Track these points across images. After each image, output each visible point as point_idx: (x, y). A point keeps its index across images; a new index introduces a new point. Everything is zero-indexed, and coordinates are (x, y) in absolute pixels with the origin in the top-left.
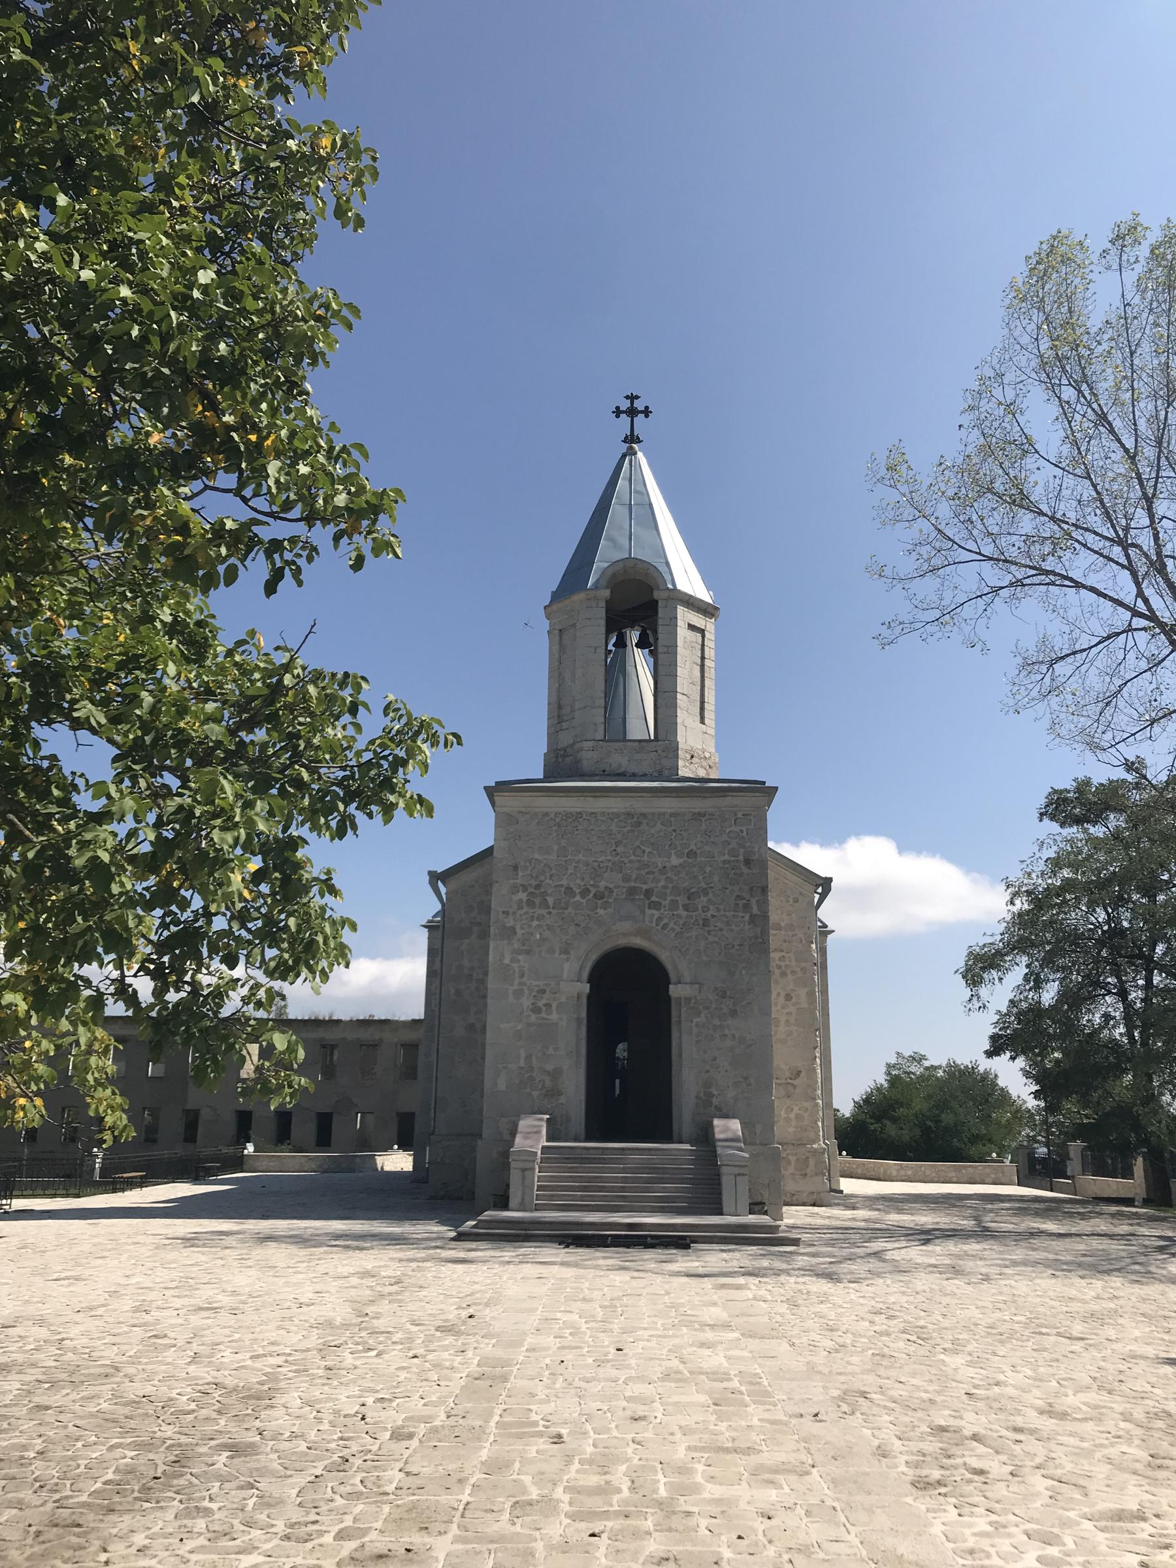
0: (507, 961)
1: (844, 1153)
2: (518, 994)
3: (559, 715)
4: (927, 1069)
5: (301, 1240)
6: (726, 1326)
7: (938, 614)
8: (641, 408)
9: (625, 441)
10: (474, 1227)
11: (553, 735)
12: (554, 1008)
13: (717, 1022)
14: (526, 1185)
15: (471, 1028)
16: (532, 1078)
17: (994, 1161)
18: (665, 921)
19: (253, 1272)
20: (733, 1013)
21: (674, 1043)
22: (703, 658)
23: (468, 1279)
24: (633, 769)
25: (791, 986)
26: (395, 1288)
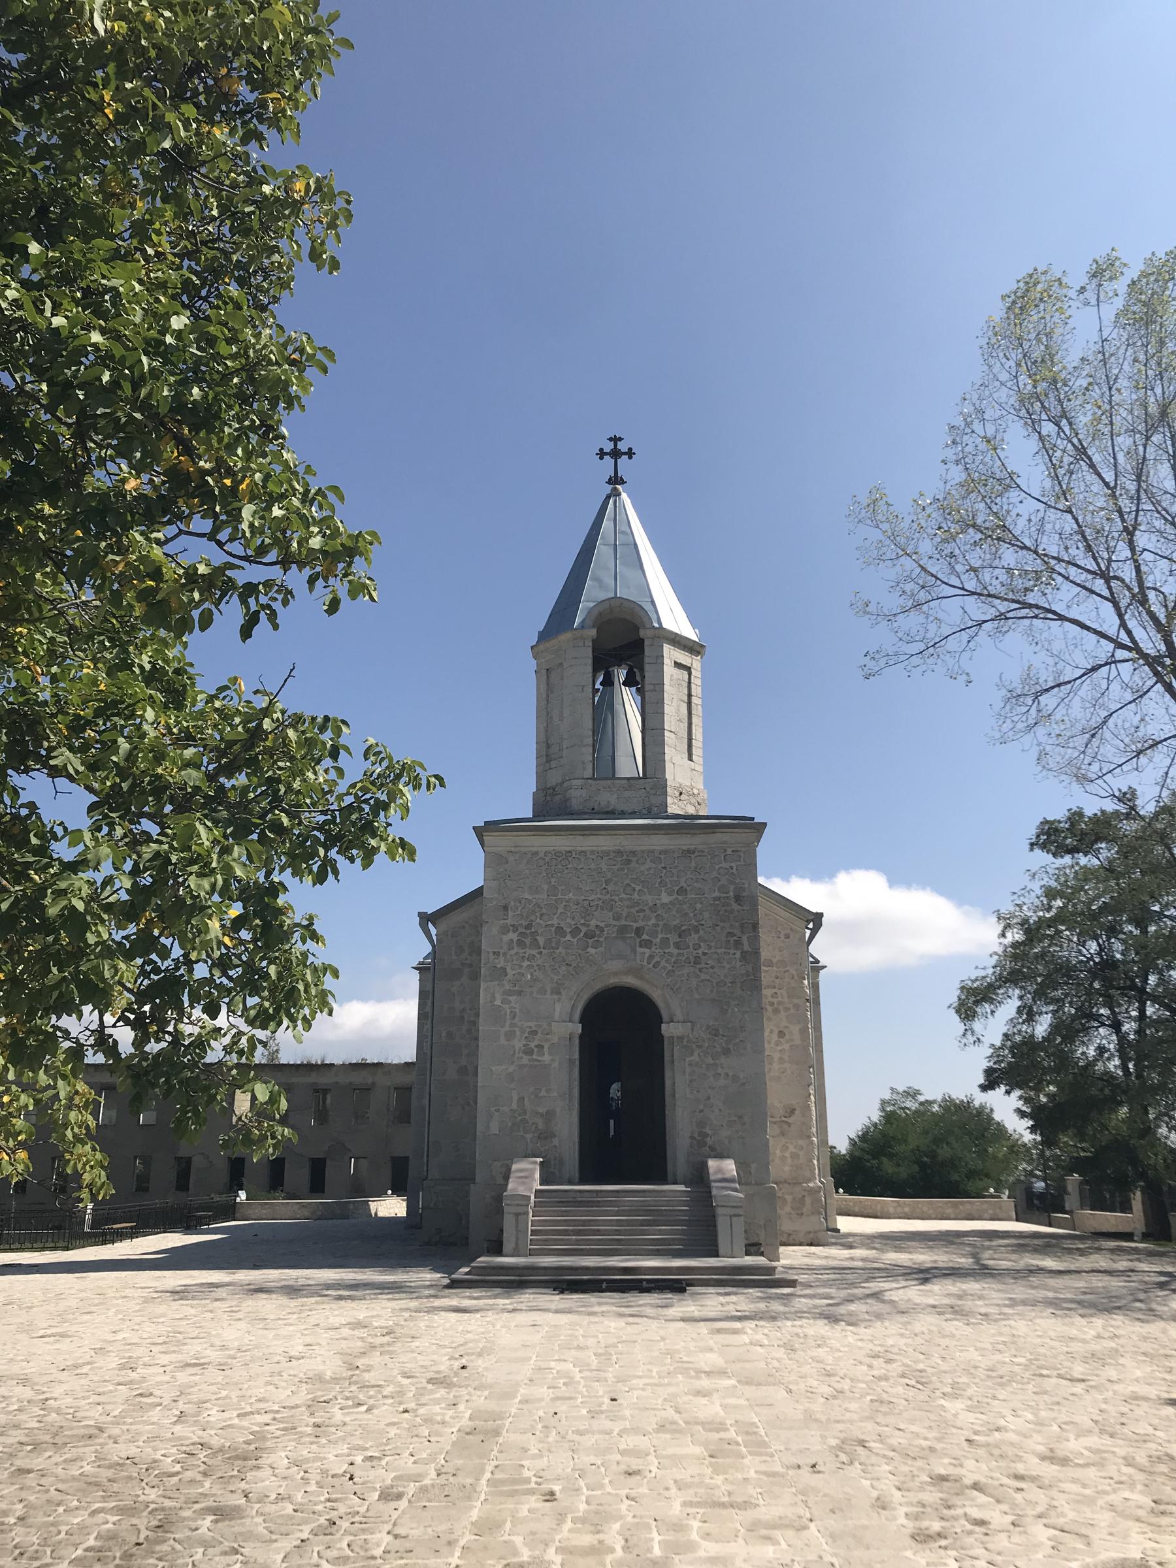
0: (498, 1002)
1: (841, 1190)
2: (510, 1035)
3: (547, 754)
4: (921, 1104)
5: (292, 1291)
6: (722, 1373)
7: (922, 647)
8: (625, 450)
9: (609, 482)
10: (467, 1273)
11: (541, 775)
12: (546, 1049)
13: (710, 1060)
14: (520, 1231)
15: (463, 1070)
16: (524, 1121)
17: (992, 1196)
18: (657, 959)
19: (242, 1325)
20: (726, 1052)
21: (668, 1082)
22: (690, 695)
23: (461, 1328)
24: (620, 807)
25: (784, 1023)
26: (387, 1339)
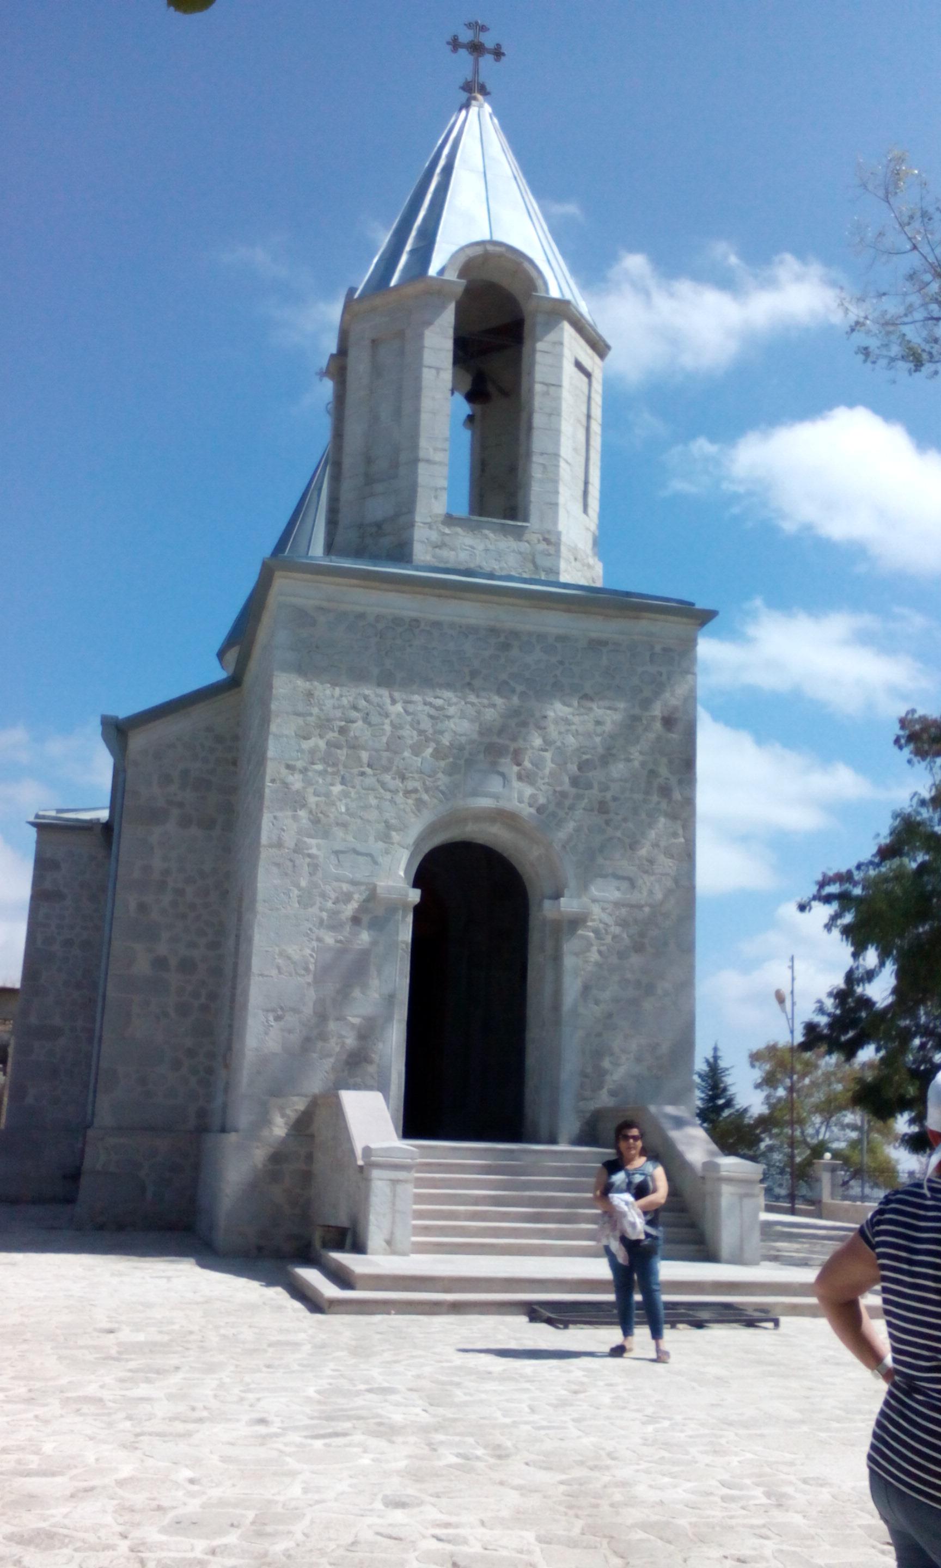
15: (160, 963)
22: (589, 417)
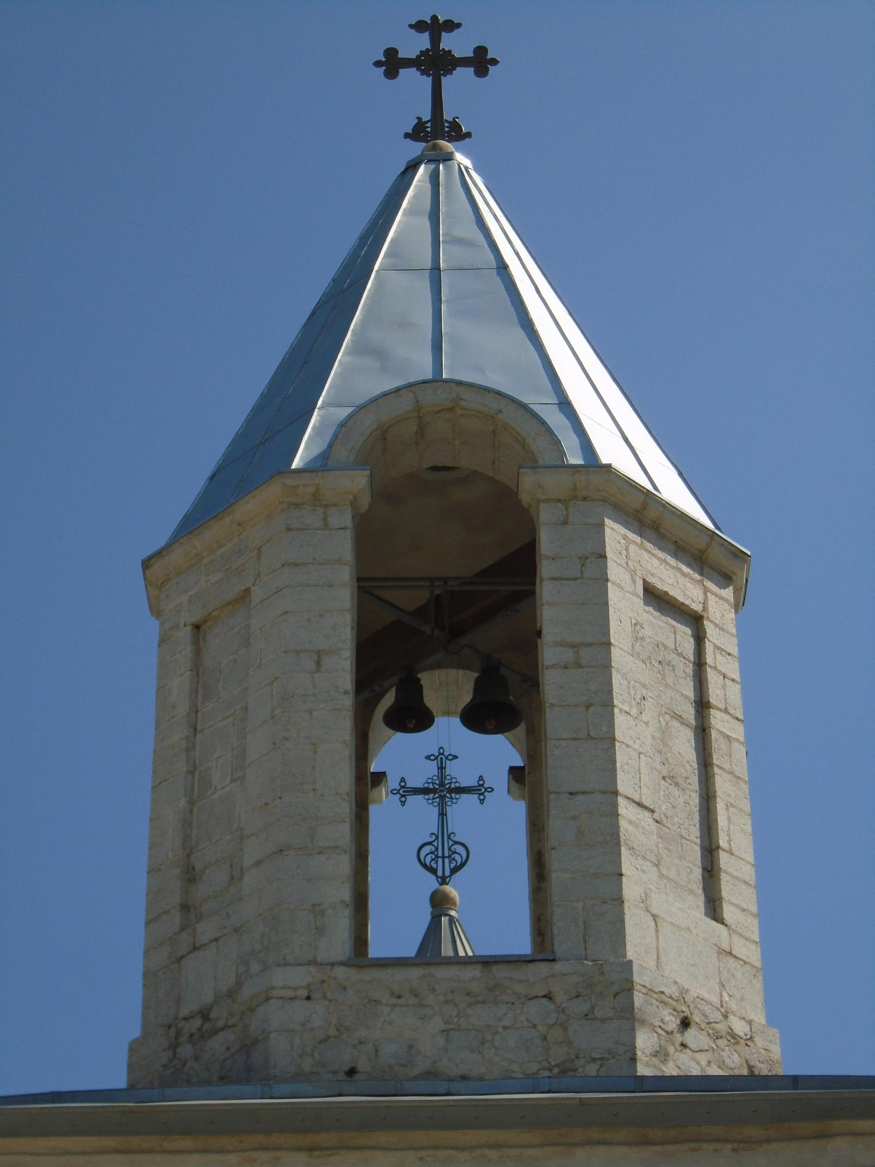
22: (702, 705)
